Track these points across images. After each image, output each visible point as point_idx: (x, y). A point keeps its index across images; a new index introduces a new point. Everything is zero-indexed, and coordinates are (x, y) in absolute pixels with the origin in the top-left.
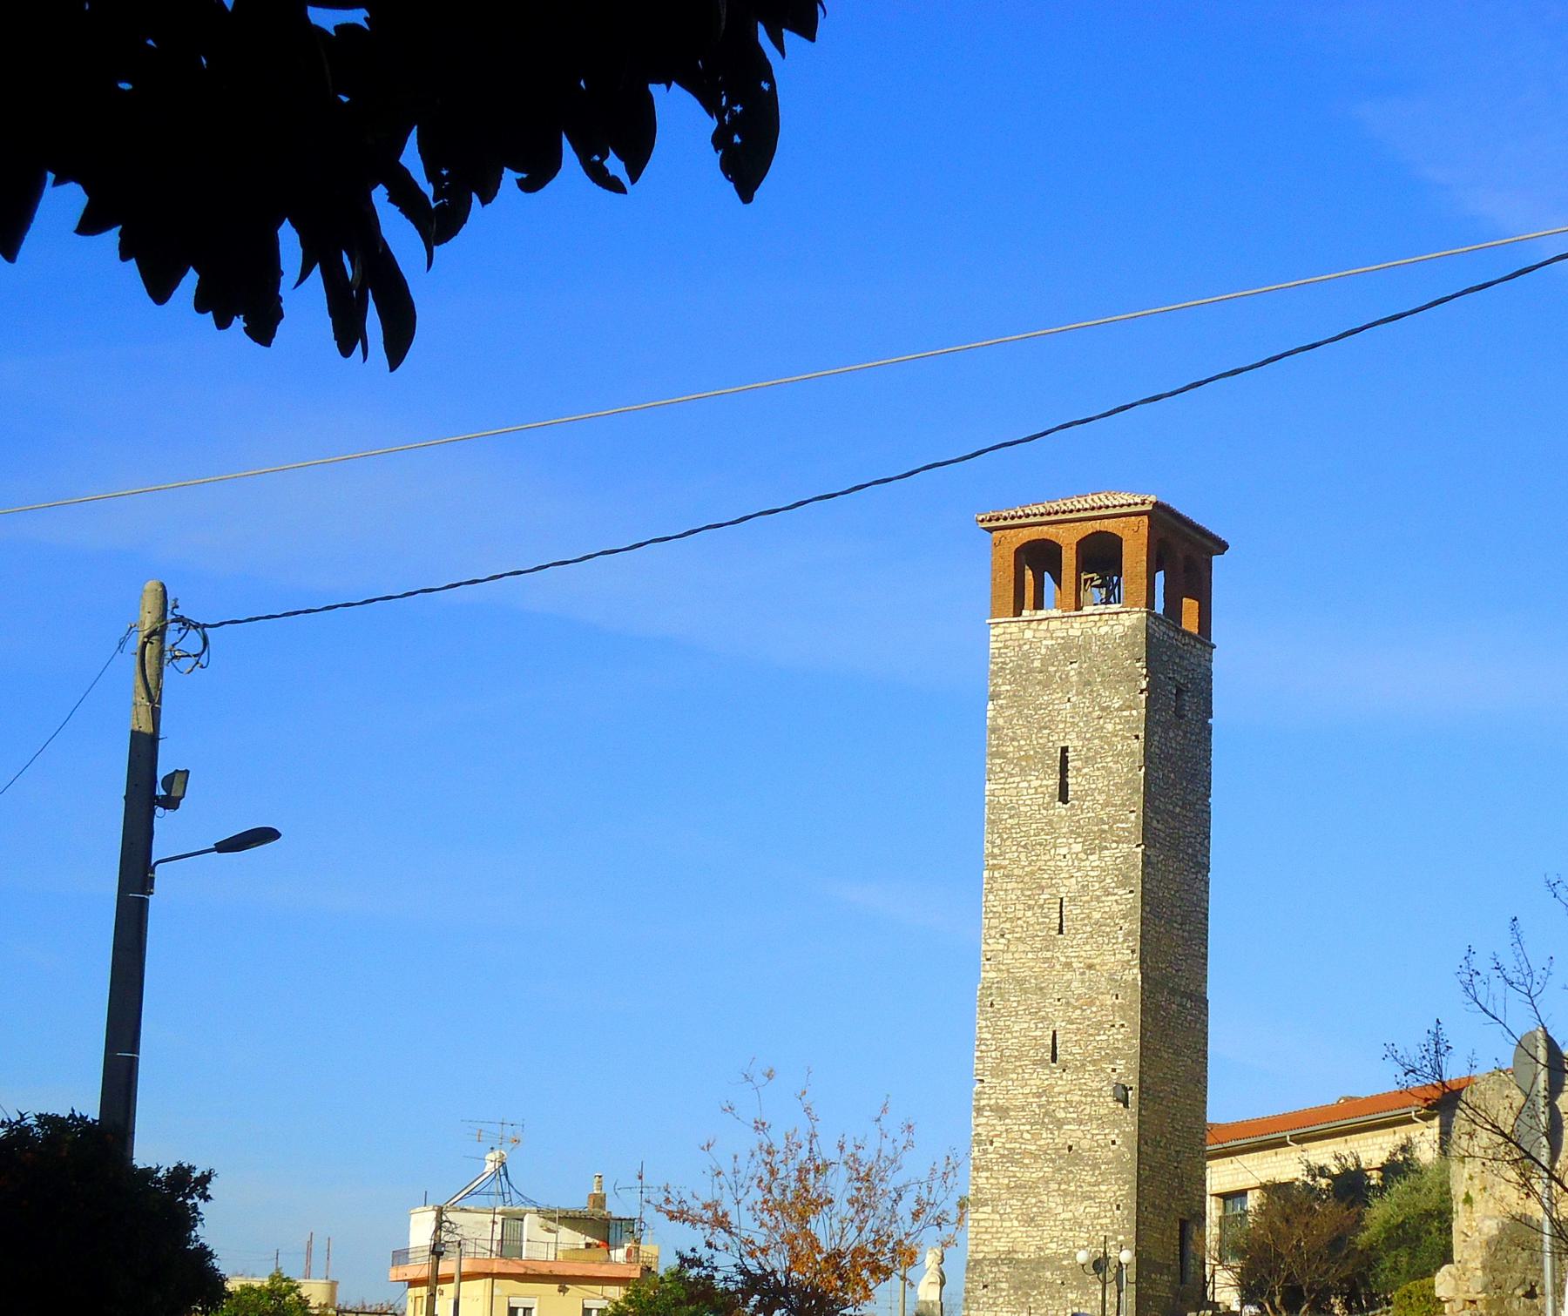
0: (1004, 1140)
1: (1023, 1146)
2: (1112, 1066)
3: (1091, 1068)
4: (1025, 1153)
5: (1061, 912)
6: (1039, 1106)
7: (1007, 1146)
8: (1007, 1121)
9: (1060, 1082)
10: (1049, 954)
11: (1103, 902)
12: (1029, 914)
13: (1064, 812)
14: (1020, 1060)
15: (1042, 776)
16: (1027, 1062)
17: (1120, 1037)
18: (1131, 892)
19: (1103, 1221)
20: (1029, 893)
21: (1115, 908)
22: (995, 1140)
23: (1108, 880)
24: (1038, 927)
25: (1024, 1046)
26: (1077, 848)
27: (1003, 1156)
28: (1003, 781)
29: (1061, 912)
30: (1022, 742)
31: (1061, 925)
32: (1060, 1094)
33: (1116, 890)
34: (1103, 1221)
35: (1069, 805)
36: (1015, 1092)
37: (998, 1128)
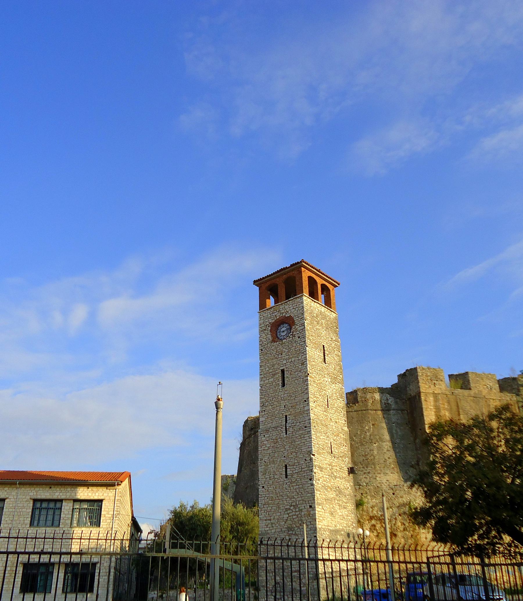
0: (322, 480)
1: (327, 484)
2: (345, 460)
3: (340, 459)
4: (328, 486)
5: (328, 400)
6: (330, 470)
7: (324, 483)
8: (323, 473)
9: (334, 462)
10: (326, 414)
11: (337, 401)
12: (320, 397)
13: (325, 367)
14: (323, 450)
15: (320, 352)
16: (325, 452)
17: (346, 450)
18: (343, 401)
19: (350, 518)
20: (320, 390)
21: (340, 405)
22: (320, 479)
23: (337, 395)
24: (323, 403)
25: (324, 445)
26: (330, 380)
27: (323, 486)
28: (311, 348)
29: (328, 400)
30: (314, 338)
31: (328, 404)
32: (334, 466)
33: (339, 399)
34: (350, 518)
35: (326, 365)
36: (323, 462)
37: (320, 475)
